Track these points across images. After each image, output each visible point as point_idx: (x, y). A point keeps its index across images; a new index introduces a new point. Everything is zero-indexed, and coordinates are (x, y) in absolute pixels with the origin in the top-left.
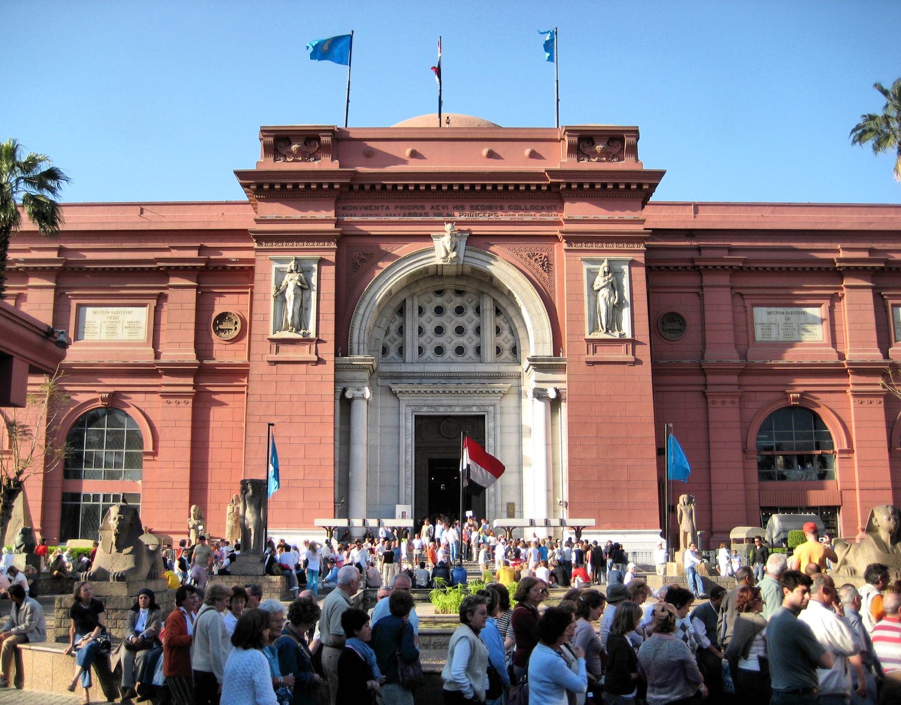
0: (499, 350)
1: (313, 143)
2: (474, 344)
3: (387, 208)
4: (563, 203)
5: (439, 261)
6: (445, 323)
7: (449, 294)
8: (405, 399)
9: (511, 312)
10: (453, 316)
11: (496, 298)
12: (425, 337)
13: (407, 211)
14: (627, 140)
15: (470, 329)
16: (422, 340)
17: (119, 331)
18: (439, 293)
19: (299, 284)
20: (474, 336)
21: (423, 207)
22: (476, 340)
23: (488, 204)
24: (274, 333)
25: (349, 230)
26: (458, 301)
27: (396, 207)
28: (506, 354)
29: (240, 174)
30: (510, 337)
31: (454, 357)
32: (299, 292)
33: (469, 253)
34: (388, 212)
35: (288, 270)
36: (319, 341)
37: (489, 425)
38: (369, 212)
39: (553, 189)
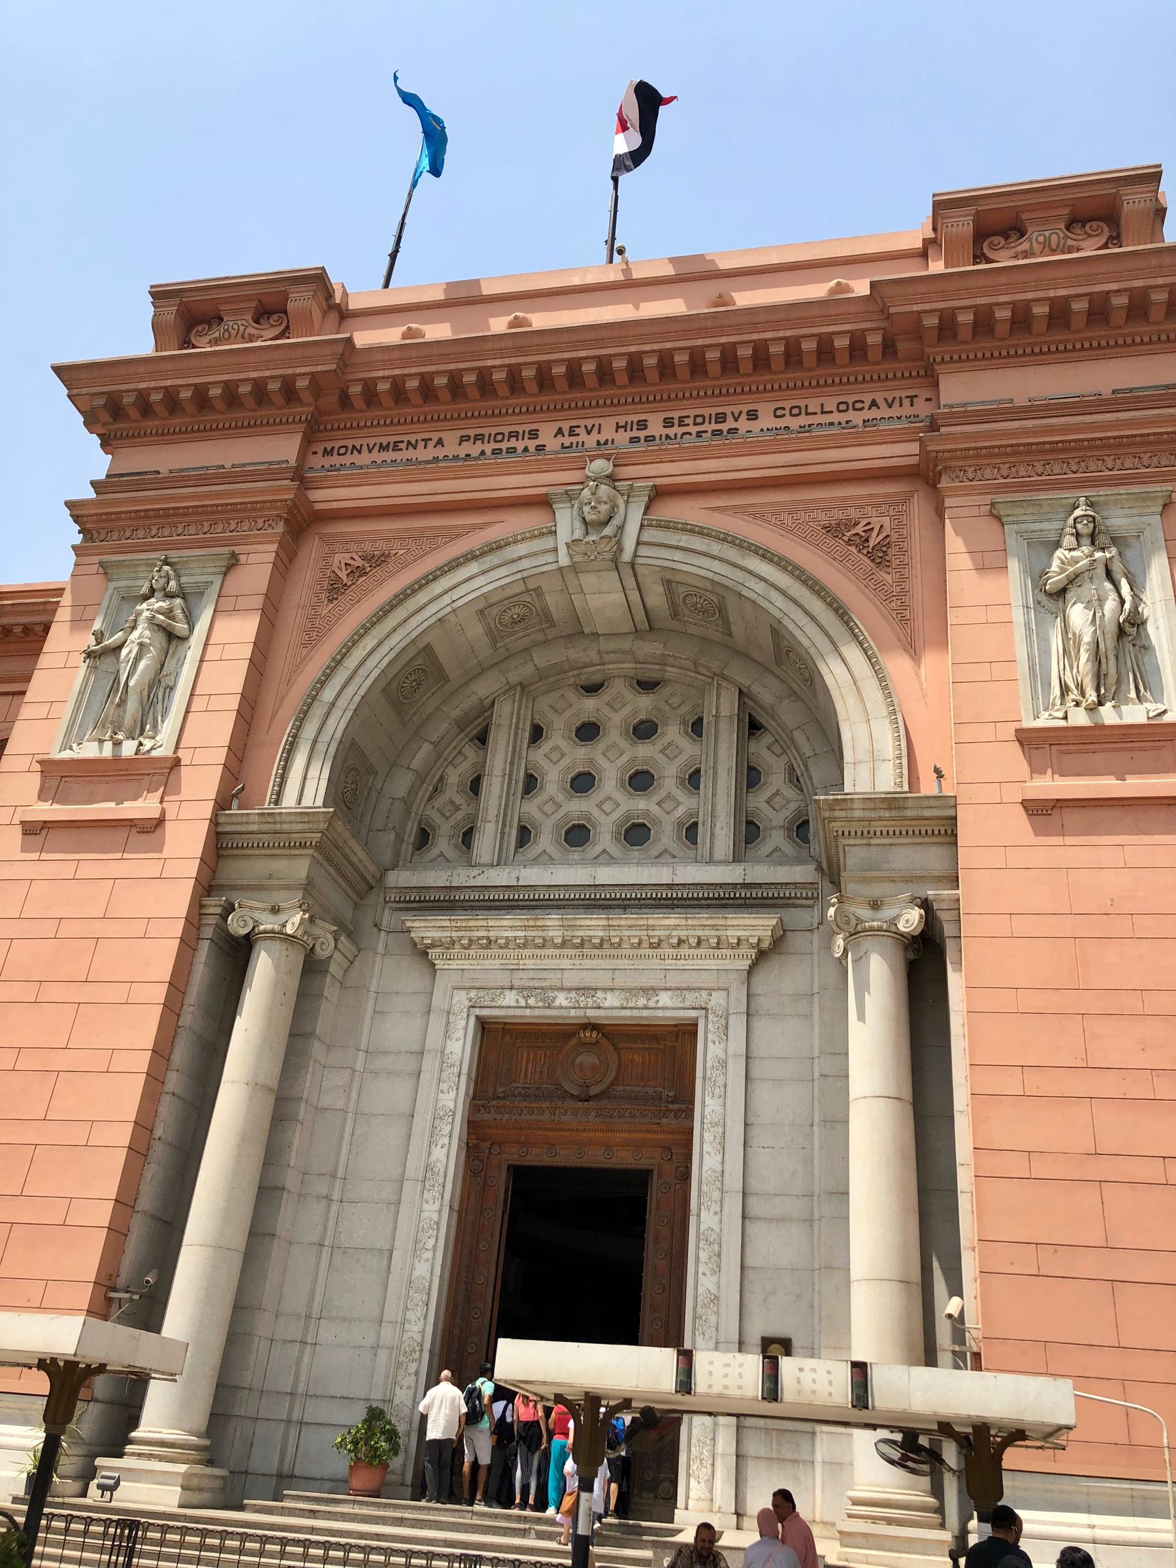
0: (749, 833)
1: (275, 317)
2: (680, 812)
3: (440, 442)
5: (564, 560)
6: (601, 760)
7: (619, 688)
8: (451, 966)
9: (788, 713)
10: (623, 743)
11: (745, 681)
12: (539, 800)
13: (488, 448)
14: (1133, 202)
15: (669, 774)
16: (531, 808)
18: (592, 689)
21: (534, 434)
22: (685, 804)
23: (714, 411)
24: (66, 746)
25: (324, 497)
26: (643, 705)
27: (463, 439)
28: (776, 839)
29: (61, 371)
30: (789, 792)
31: (614, 850)
32: (160, 638)
33: (650, 535)
35: (145, 590)
38: (389, 456)
39: (903, 346)
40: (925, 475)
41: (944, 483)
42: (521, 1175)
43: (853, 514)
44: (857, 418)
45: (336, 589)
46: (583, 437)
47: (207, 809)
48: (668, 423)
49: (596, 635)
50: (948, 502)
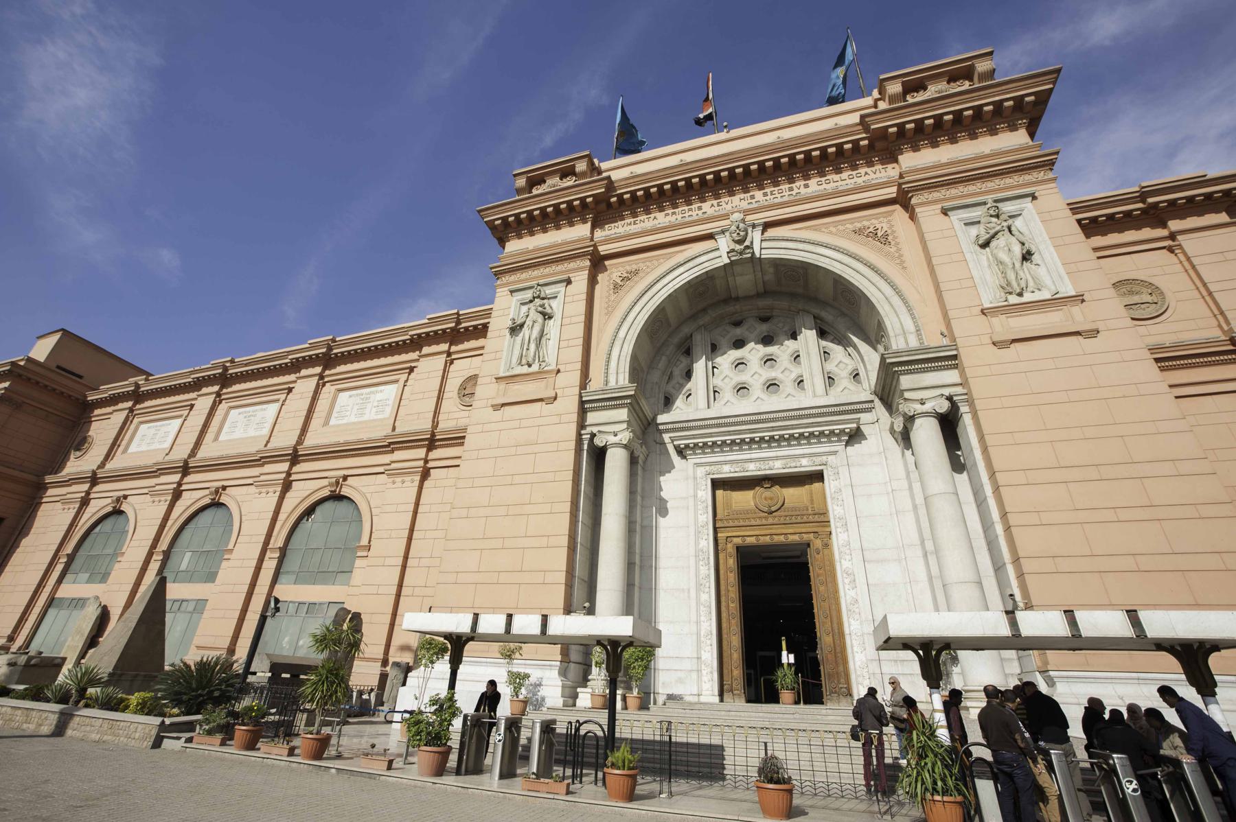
2: (793, 376)
4: (896, 161)
17: (367, 411)
18: (737, 324)
19: (540, 309)
20: (792, 367)
21: (700, 208)
22: (795, 371)
26: (764, 328)
32: (540, 318)
33: (765, 244)
34: (656, 222)
36: (559, 371)
37: (830, 484)
38: (633, 227)
39: (879, 145)
40: (903, 199)
41: (913, 201)
42: (743, 553)
43: (866, 223)
44: (860, 181)
45: (617, 287)
46: (724, 205)
47: (577, 390)
48: (765, 195)
49: (737, 299)
50: (917, 210)
